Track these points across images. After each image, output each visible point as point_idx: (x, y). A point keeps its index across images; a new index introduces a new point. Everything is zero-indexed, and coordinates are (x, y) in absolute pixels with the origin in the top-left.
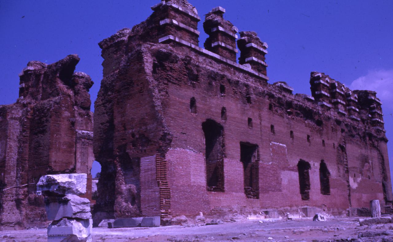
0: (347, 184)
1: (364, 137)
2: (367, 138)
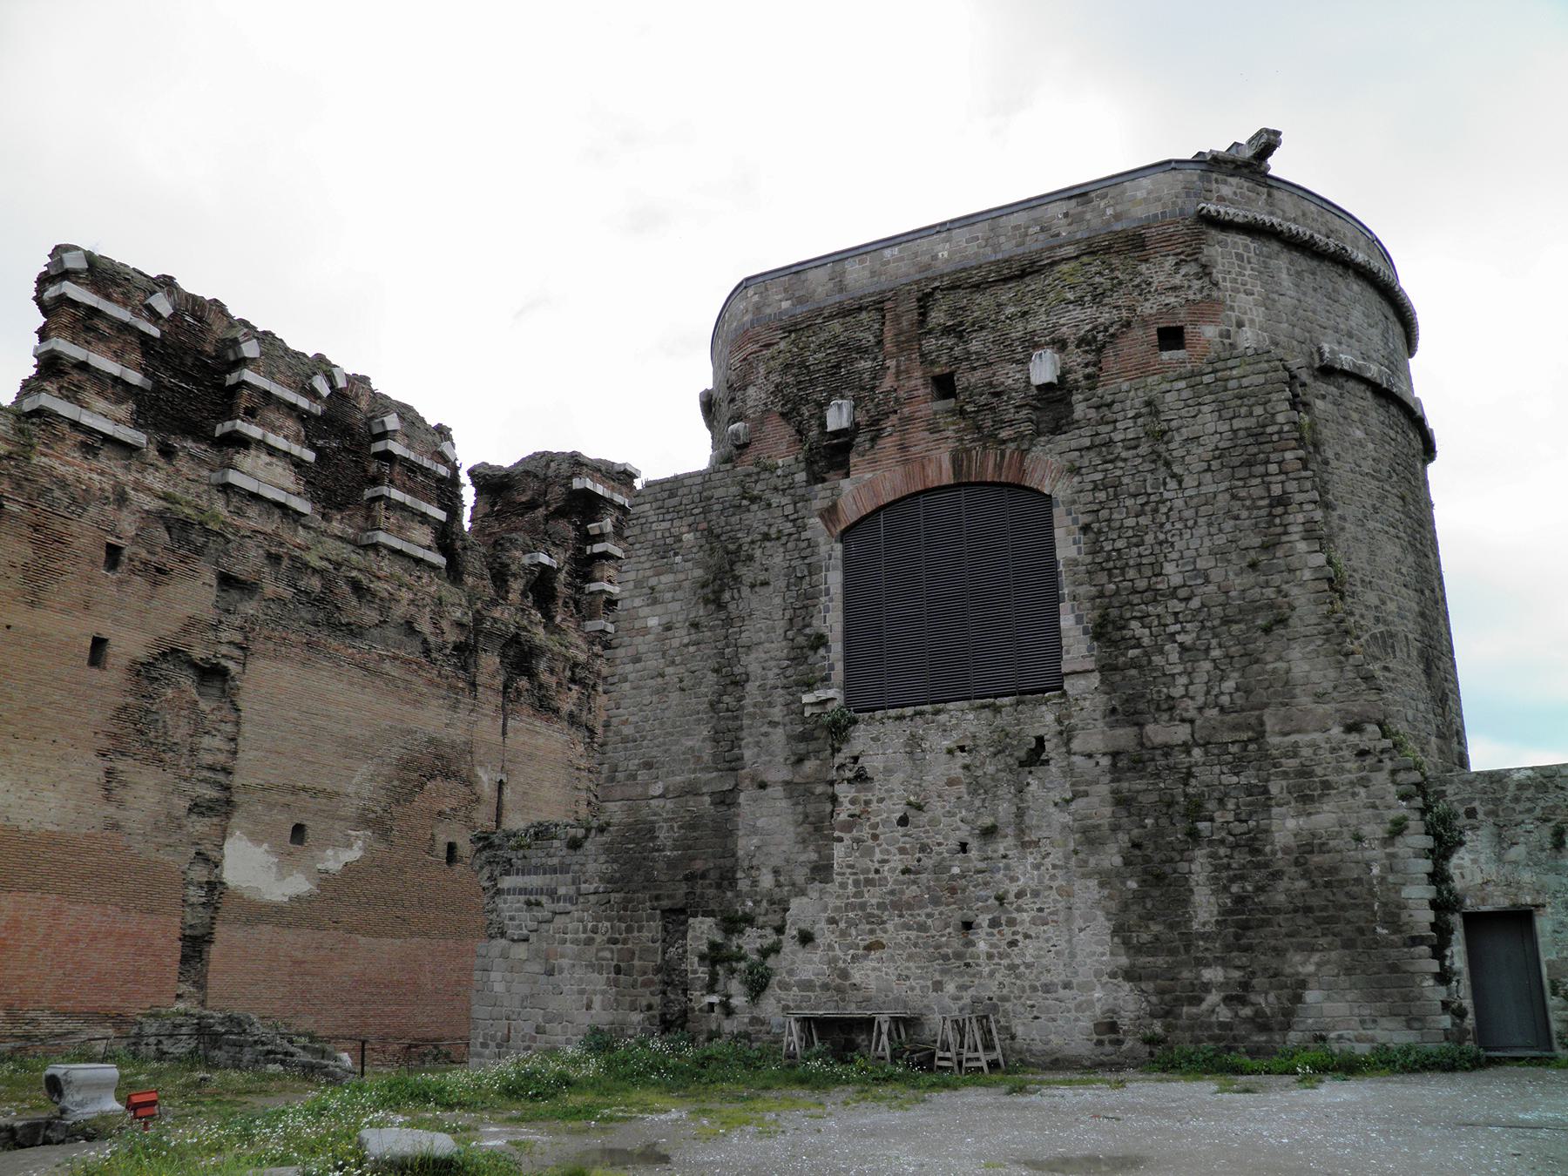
0: (200, 873)
1: (465, 652)
2: (489, 663)
